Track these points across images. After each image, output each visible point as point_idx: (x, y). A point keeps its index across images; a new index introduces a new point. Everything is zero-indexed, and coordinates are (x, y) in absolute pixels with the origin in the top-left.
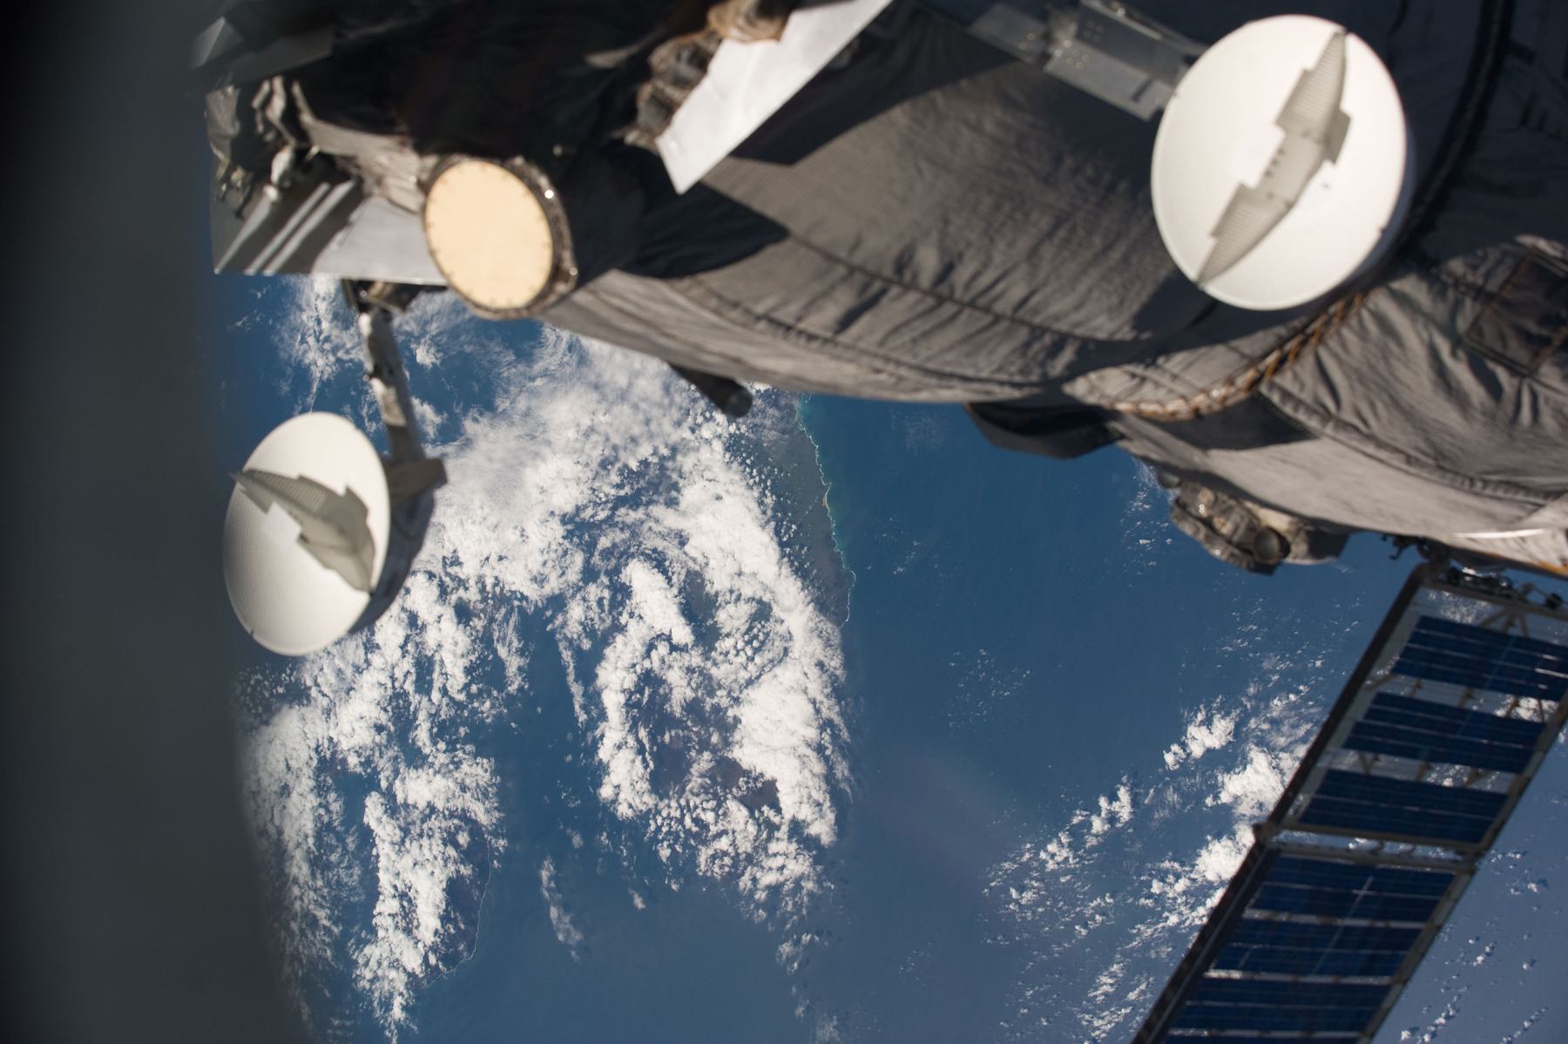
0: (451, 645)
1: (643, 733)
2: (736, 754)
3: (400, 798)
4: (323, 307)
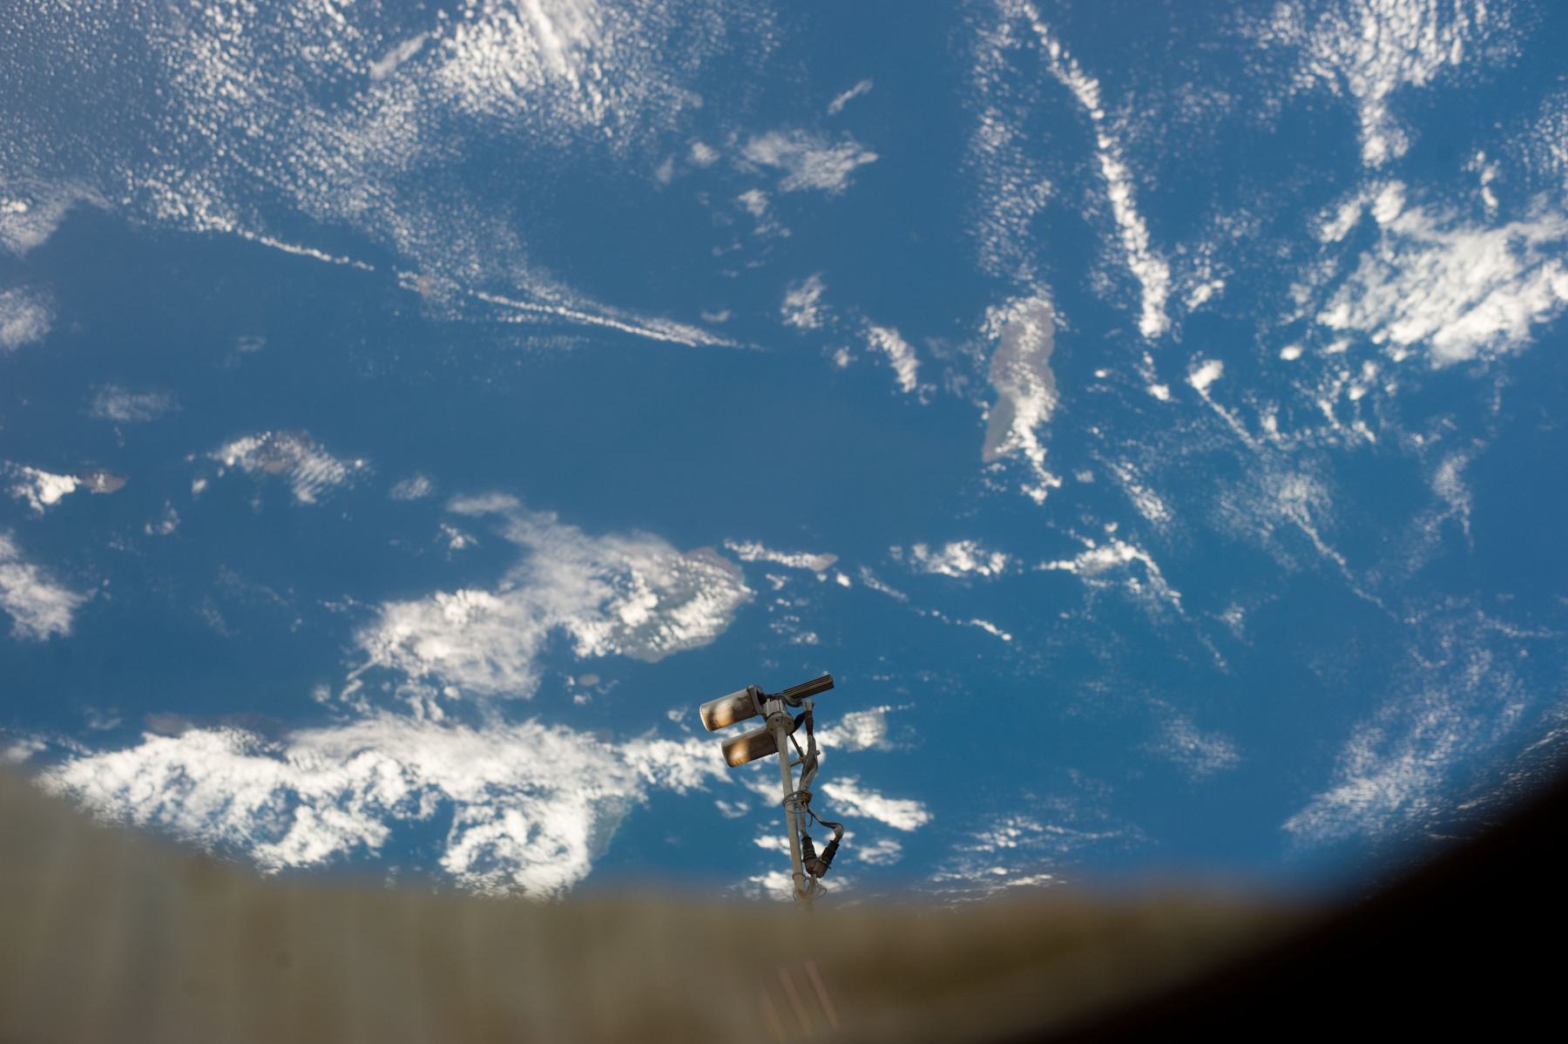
0: (392, 790)
1: (474, 857)
2: (516, 876)
3: (325, 815)
4: (396, 639)
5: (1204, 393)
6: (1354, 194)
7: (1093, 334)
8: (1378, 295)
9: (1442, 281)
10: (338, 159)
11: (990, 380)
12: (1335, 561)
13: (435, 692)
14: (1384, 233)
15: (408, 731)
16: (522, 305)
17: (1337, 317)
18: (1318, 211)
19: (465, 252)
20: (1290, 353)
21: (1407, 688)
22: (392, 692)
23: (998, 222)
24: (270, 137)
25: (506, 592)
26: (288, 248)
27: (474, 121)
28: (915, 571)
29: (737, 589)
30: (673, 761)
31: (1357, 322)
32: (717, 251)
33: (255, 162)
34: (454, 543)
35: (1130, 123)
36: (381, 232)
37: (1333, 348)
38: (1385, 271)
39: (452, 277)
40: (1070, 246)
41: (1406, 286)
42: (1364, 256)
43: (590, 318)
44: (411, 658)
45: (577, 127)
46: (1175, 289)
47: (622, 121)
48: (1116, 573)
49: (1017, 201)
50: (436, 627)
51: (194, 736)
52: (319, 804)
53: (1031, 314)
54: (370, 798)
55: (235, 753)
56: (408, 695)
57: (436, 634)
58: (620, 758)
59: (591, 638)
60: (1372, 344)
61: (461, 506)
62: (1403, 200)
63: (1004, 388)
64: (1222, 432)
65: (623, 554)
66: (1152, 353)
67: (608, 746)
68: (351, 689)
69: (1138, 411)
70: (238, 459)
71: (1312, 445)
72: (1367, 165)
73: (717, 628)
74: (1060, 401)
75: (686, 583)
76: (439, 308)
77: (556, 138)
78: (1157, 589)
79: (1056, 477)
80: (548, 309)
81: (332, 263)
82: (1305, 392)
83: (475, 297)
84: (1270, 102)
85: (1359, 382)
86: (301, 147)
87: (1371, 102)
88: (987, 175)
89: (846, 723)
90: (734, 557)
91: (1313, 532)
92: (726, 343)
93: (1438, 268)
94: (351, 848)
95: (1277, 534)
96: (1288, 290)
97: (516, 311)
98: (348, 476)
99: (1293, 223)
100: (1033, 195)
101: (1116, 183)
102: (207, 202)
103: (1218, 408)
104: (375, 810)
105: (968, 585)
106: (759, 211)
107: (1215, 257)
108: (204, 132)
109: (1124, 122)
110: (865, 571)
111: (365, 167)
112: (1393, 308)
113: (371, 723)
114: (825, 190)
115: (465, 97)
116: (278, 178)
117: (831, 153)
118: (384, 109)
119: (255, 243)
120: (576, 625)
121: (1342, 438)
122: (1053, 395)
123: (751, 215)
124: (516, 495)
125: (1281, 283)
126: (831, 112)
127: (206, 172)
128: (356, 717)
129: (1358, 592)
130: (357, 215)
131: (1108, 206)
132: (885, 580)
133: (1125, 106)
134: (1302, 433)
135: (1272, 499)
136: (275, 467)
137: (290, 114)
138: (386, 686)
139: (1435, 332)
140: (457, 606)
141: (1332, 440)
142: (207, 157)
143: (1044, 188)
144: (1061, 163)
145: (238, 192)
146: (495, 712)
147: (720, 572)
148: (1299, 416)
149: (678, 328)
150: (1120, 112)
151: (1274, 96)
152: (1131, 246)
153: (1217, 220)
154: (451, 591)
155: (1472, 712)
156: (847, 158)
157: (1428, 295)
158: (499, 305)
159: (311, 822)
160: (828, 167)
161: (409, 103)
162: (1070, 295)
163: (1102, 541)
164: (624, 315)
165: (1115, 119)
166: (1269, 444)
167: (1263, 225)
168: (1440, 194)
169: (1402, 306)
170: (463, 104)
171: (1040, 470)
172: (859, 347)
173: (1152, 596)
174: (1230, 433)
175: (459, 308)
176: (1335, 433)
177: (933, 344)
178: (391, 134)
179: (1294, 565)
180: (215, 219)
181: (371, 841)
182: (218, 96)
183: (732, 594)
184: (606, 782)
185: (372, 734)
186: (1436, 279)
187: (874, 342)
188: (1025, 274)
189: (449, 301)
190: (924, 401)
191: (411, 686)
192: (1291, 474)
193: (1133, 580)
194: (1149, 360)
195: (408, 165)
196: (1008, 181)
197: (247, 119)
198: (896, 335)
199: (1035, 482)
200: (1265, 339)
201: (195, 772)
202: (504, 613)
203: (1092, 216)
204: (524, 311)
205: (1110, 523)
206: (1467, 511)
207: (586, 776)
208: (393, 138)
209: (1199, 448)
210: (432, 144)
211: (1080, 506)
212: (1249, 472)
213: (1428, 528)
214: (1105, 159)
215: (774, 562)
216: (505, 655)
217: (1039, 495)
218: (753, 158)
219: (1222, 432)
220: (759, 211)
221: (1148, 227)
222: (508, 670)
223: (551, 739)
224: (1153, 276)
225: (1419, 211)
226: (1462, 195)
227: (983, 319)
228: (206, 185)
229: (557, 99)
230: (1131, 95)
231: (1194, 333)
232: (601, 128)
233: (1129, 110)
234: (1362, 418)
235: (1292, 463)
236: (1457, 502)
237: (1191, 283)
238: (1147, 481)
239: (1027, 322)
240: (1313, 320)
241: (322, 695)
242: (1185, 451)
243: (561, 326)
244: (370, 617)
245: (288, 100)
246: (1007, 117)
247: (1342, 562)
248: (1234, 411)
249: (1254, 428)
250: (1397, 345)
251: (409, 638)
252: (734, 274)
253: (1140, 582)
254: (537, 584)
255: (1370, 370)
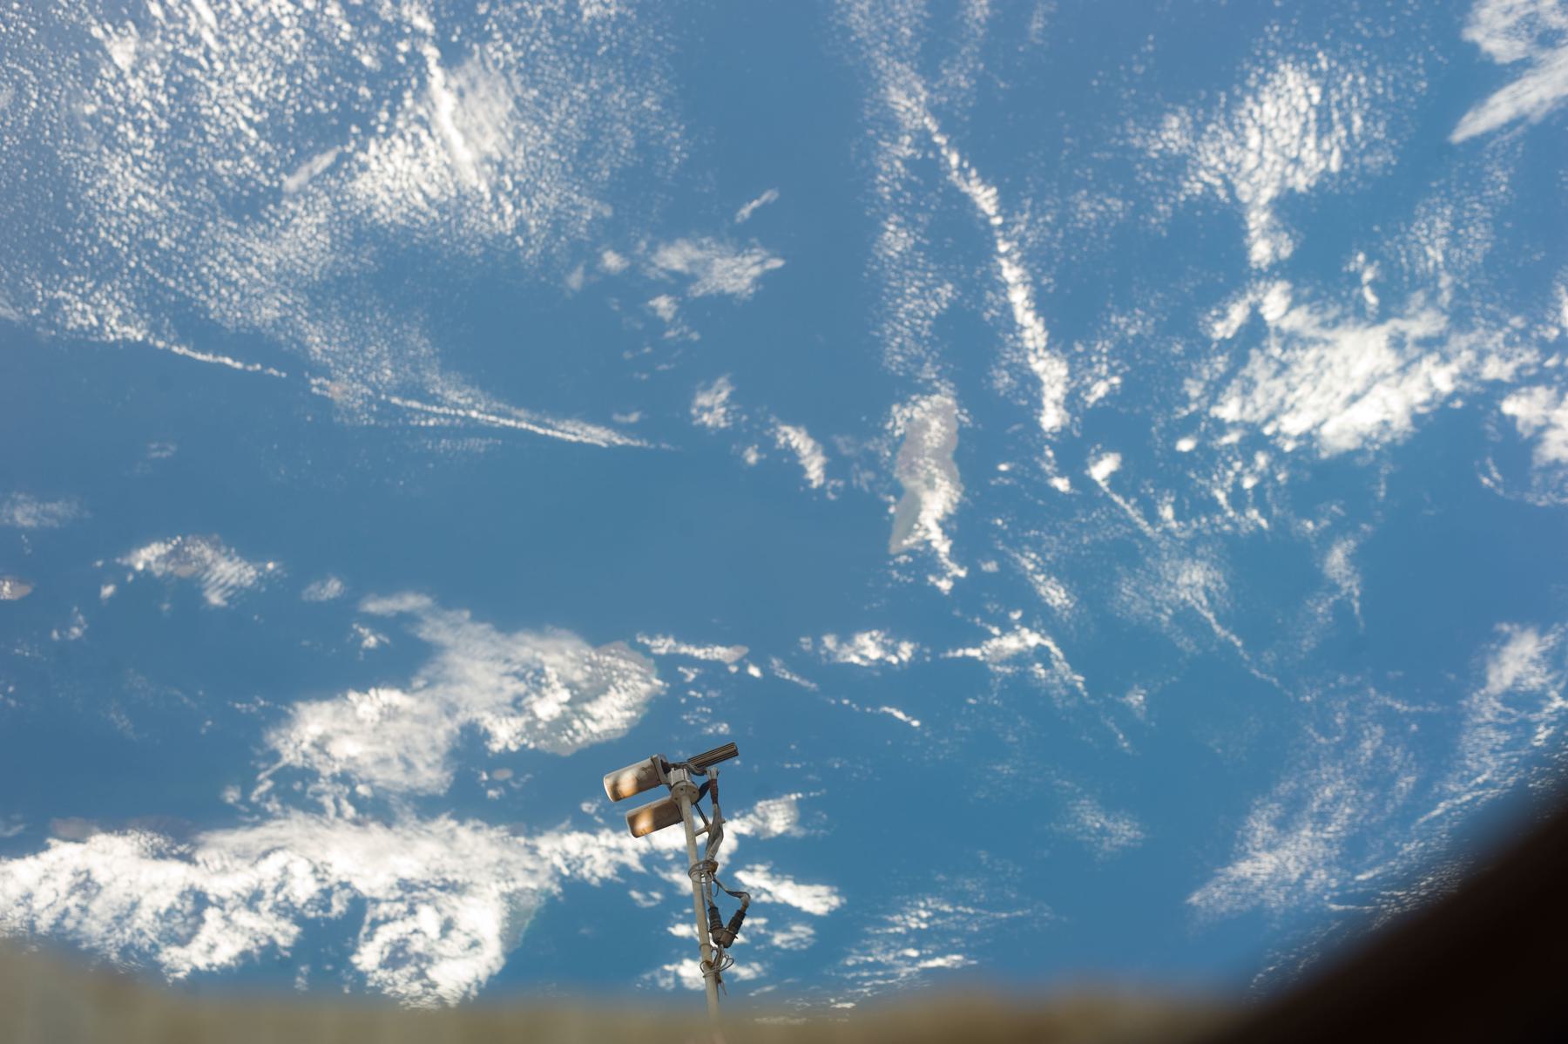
0: (303, 889)
3: (235, 916)
4: (308, 739)
5: (1103, 485)
6: (1243, 294)
7: (995, 431)
8: (1268, 390)
9: (1328, 375)
10: (251, 270)
11: (896, 475)
12: (1232, 643)
13: (347, 790)
14: (1272, 330)
15: (319, 830)
16: (435, 409)
17: (1229, 410)
18: (1209, 310)
19: (378, 358)
20: (1185, 445)
21: (1303, 763)
22: (304, 792)
23: (902, 324)
24: (182, 249)
25: (419, 690)
26: (199, 356)
27: (386, 231)
28: (825, 660)
29: (649, 682)
30: (586, 853)
31: (1249, 415)
32: (627, 355)
33: (167, 273)
34: (366, 643)
35: (1028, 229)
36: (293, 340)
37: (1226, 440)
38: (1274, 367)
39: (364, 382)
40: (971, 345)
41: (1294, 380)
42: (1254, 352)
43: (502, 421)
44: (323, 757)
45: (489, 237)
46: (1073, 385)
47: (534, 230)
48: (1021, 659)
49: (920, 303)
50: (348, 726)
51: (100, 841)
52: (229, 905)
53: (935, 412)
54: (280, 897)
55: (142, 857)
56: (320, 794)
57: (348, 733)
58: (533, 850)
59: (505, 733)
60: (1262, 435)
61: (373, 607)
62: (1289, 299)
63: (910, 483)
64: (1121, 521)
65: (536, 650)
66: (1053, 446)
67: (521, 840)
68: (262, 789)
69: (1040, 502)
70: (147, 564)
71: (1208, 532)
72: (1254, 266)
73: (629, 721)
74: (965, 494)
75: (599, 676)
76: (351, 413)
77: (468, 247)
78: (1062, 674)
79: (961, 567)
80: (461, 412)
81: (244, 370)
82: (1200, 481)
83: (388, 402)
84: (1161, 208)
85: (1252, 472)
86: (213, 258)
87: (1257, 207)
88: (890, 279)
89: (758, 810)
90: (646, 651)
91: (1210, 616)
92: (638, 443)
93: (1324, 362)
94: (261, 948)
95: (1176, 618)
96: (1182, 385)
97: (428, 415)
98: (260, 579)
99: (1184, 322)
100: (936, 297)
101: (1015, 285)
102: (118, 312)
103: (1118, 499)
104: (285, 910)
105: (877, 674)
106: (668, 316)
107: (1112, 355)
108: (115, 244)
109: (1022, 227)
110: (775, 662)
111: (278, 277)
112: (1282, 401)
113: (281, 822)
114: (733, 295)
115: (377, 209)
116: (189, 288)
117: (739, 259)
118: (296, 220)
119: (167, 352)
120: (489, 721)
121: (1236, 526)
122: (958, 489)
123: (661, 320)
124: (429, 594)
125: (1176, 378)
126: (739, 220)
127: (117, 283)
128: (267, 817)
129: (1255, 672)
130: (269, 324)
131: (1008, 308)
132: (795, 669)
133: (1022, 212)
134: (1199, 522)
135: (1170, 585)
136: (185, 571)
137: (202, 226)
138: (298, 786)
139: (1322, 423)
140: (370, 704)
141: (1227, 527)
142: (118, 268)
143: (946, 291)
144: (962, 267)
145: (149, 301)
146: (407, 809)
147: (632, 666)
148: (1195, 505)
149: (590, 429)
150: (1018, 217)
151: (1165, 202)
152: (1030, 345)
153: (1113, 319)
154: (363, 688)
155: (1367, 785)
156: (755, 264)
157: (1315, 388)
158: (411, 409)
159: (220, 924)
160: (736, 273)
161: (322, 214)
162: (972, 392)
163: (1007, 628)
164: (536, 417)
165: (1013, 225)
166: (1167, 532)
167: (1156, 324)
168: (1324, 293)
169: (1290, 399)
170: (376, 215)
171: (946, 561)
172: (767, 444)
173: (1056, 680)
174: (1130, 523)
175: (371, 413)
176: (1229, 521)
177: (840, 441)
178: (303, 245)
179: (1193, 647)
180: (126, 329)
181: (282, 941)
182: (129, 210)
183: (645, 687)
184: (520, 875)
185: (283, 833)
186: (1322, 373)
187: (782, 440)
188: (929, 372)
189: (361, 407)
190: (832, 497)
191: (322, 785)
192: (1188, 561)
193: (1038, 665)
194: (1050, 453)
195: (321, 273)
196: (911, 284)
197: (159, 232)
198: (804, 433)
199: (941, 573)
200: (1161, 431)
201: (101, 876)
202: (416, 711)
203: (993, 317)
204: (436, 415)
205: (1015, 610)
206: (1357, 593)
207: (499, 870)
208: (305, 249)
209: (1101, 538)
210: (345, 255)
211: (986, 595)
212: (1148, 559)
213: (1320, 610)
214: (1004, 263)
215: (685, 655)
216: (418, 752)
217: (945, 585)
218: (663, 265)
219: (1121, 521)
220: (668, 316)
221: (1047, 327)
222: (421, 766)
223: (464, 834)
224: (1053, 374)
225: (1305, 309)
226: (1344, 294)
227: (889, 417)
228: (117, 295)
229: (469, 210)
230: (1028, 202)
231: (1092, 427)
232: (512, 237)
233: (1026, 216)
234: (1255, 505)
235: (1189, 550)
236: (1346, 584)
237: (1089, 379)
238: (1050, 570)
239: (931, 419)
240: (1207, 413)
241: (232, 796)
242: (1086, 540)
243: (473, 429)
244: (280, 717)
245: (201, 213)
246: (909, 223)
247: (1239, 644)
248: (1133, 501)
249: (1152, 517)
250: (1287, 436)
251: (320, 737)
252: (644, 377)
253: (1045, 667)
254: (450, 681)
255: (1261, 460)
